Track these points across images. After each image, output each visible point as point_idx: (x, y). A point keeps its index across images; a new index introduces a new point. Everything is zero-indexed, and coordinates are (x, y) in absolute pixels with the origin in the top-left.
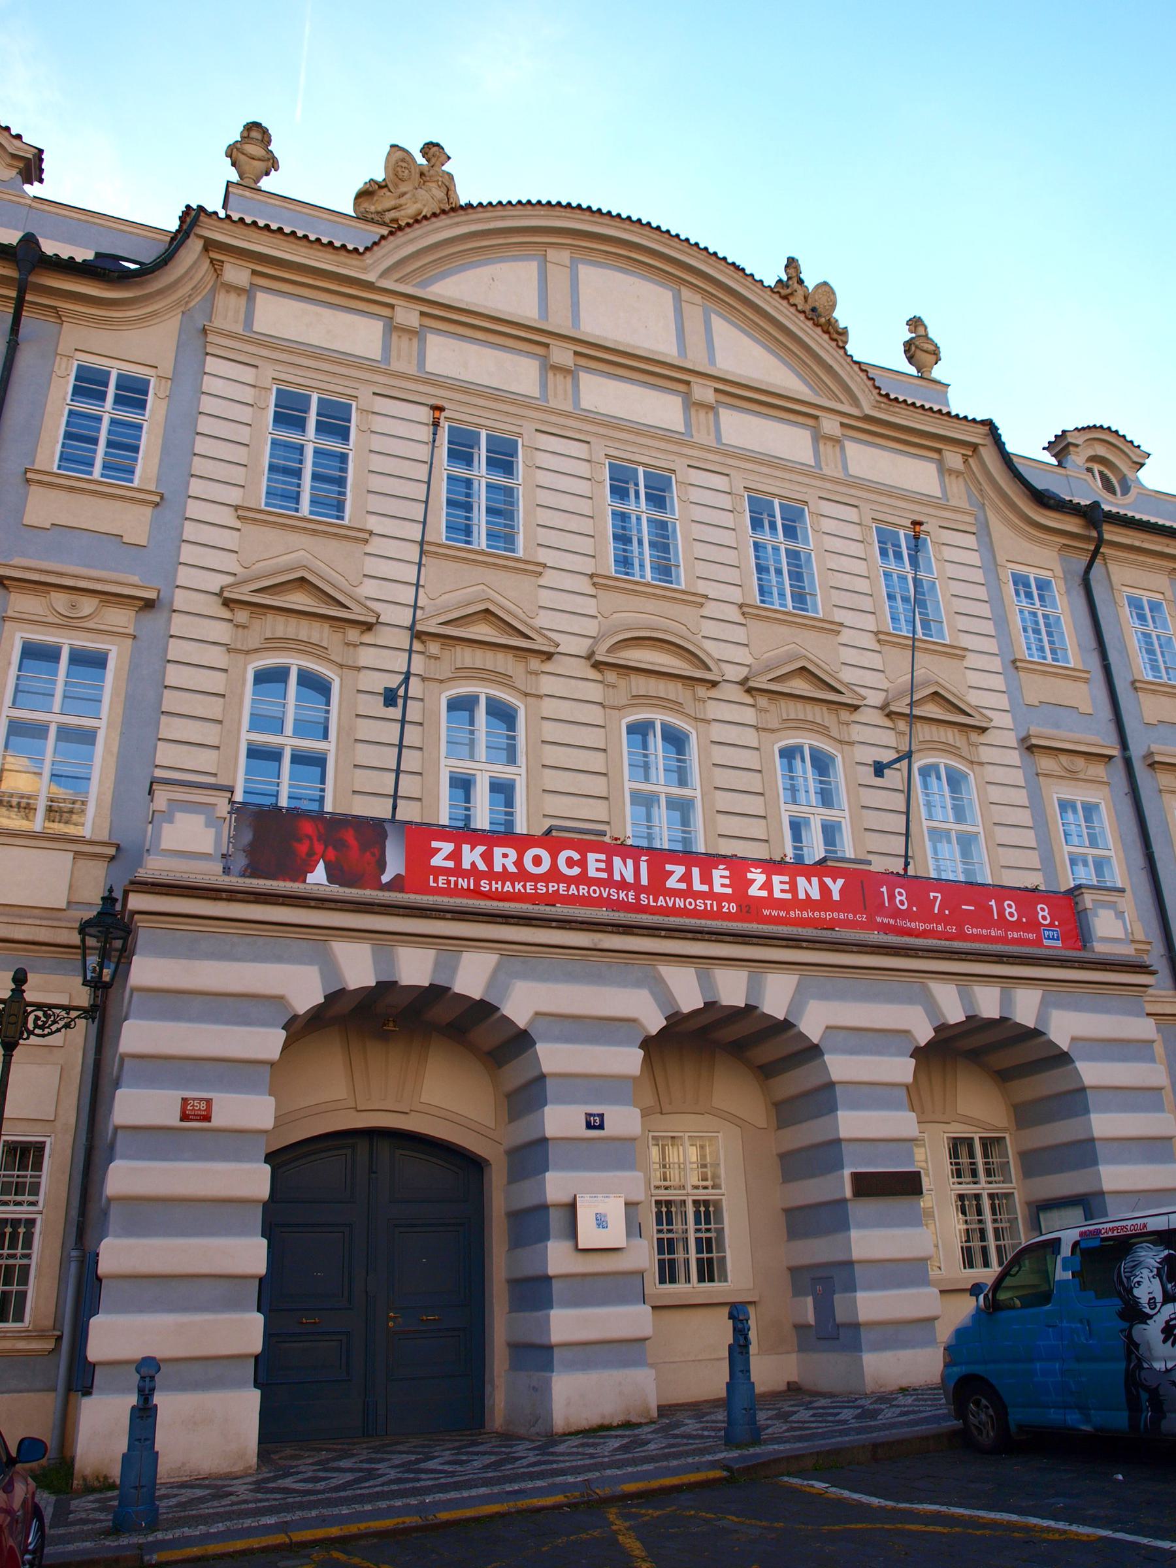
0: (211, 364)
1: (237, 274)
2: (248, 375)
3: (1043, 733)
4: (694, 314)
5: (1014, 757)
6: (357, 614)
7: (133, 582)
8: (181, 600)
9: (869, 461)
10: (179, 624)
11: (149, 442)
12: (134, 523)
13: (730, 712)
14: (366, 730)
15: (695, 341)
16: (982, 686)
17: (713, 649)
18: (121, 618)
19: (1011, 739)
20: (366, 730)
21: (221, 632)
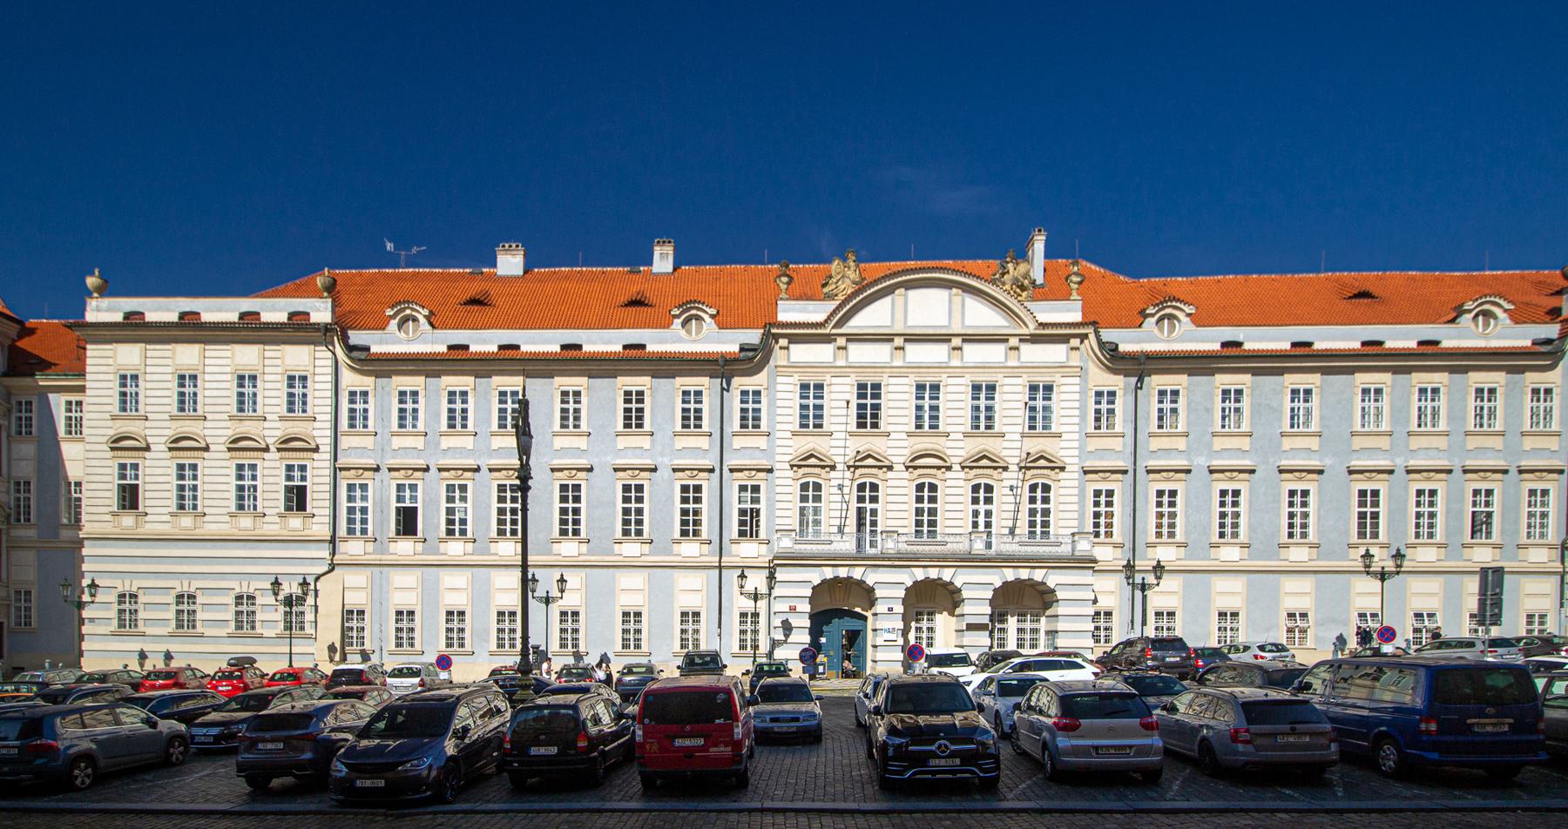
0: (779, 379)
1: (783, 342)
2: (790, 380)
3: (1091, 463)
4: (957, 300)
5: (1076, 475)
6: (829, 463)
7: (765, 463)
8: (777, 466)
9: (1032, 353)
10: (777, 473)
11: (764, 415)
12: (761, 442)
13: (957, 473)
14: (833, 498)
15: (957, 315)
16: (1067, 449)
17: (949, 452)
18: (762, 475)
19: (1076, 468)
20: (833, 498)
21: (790, 473)
